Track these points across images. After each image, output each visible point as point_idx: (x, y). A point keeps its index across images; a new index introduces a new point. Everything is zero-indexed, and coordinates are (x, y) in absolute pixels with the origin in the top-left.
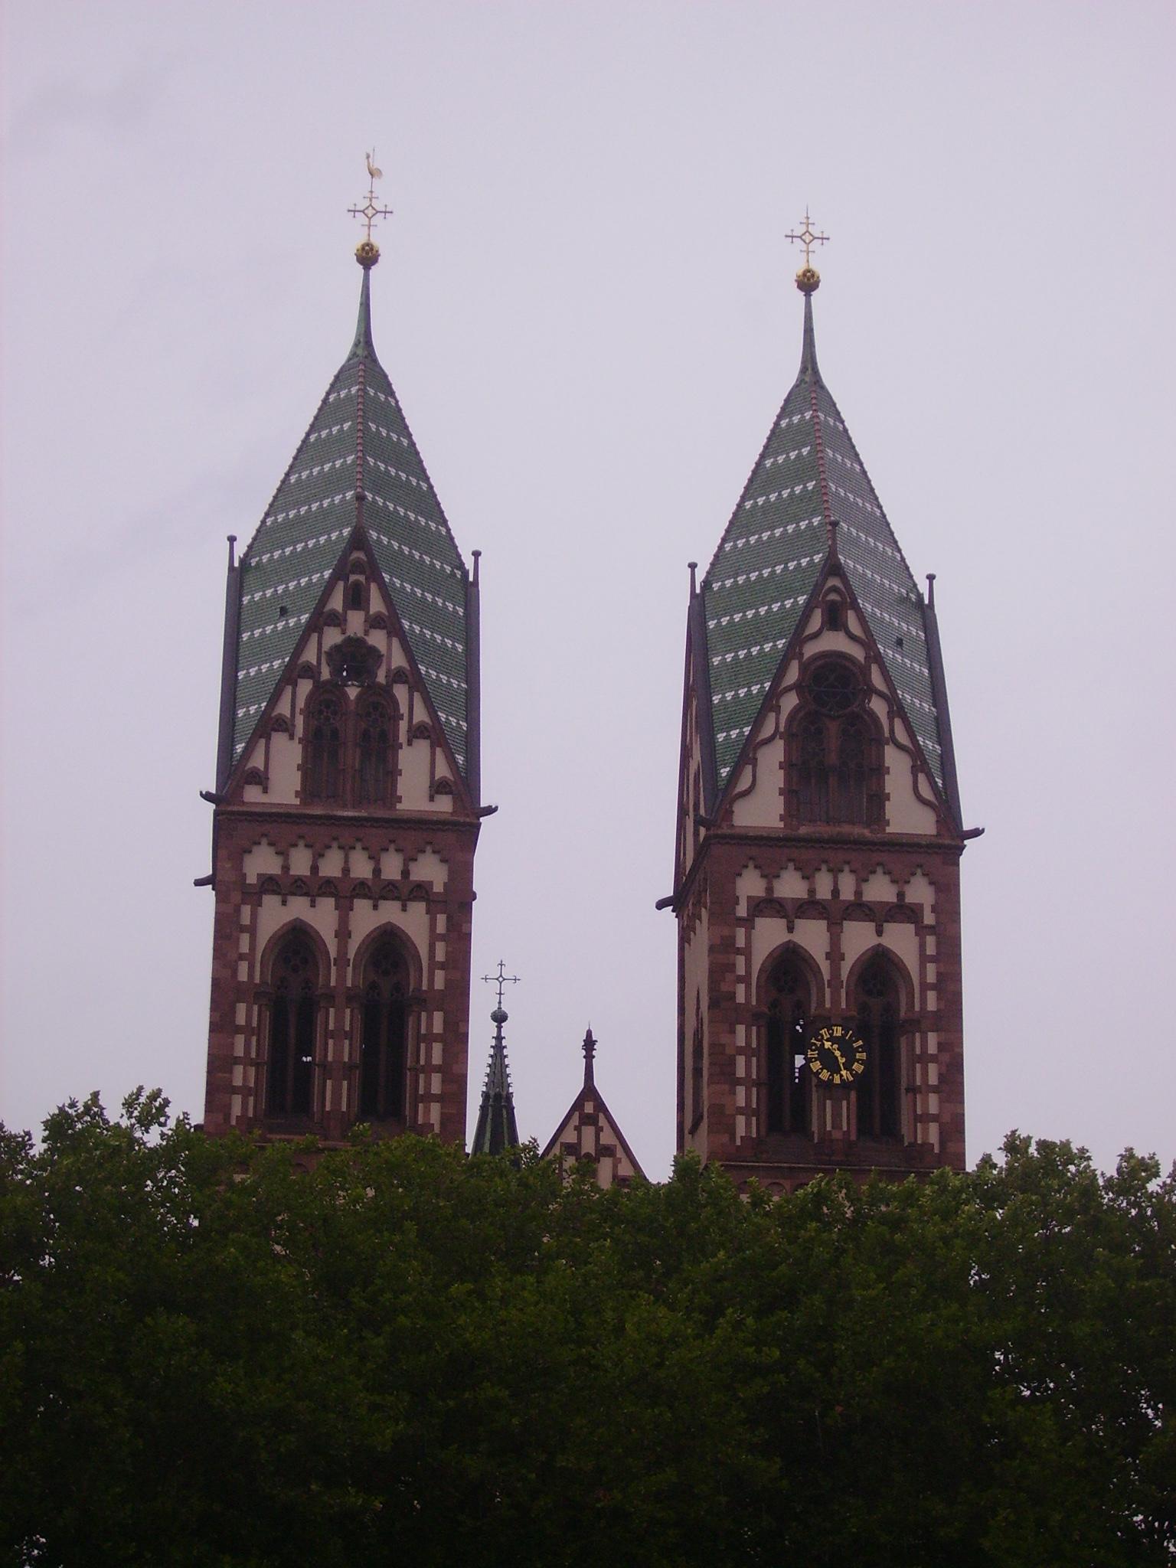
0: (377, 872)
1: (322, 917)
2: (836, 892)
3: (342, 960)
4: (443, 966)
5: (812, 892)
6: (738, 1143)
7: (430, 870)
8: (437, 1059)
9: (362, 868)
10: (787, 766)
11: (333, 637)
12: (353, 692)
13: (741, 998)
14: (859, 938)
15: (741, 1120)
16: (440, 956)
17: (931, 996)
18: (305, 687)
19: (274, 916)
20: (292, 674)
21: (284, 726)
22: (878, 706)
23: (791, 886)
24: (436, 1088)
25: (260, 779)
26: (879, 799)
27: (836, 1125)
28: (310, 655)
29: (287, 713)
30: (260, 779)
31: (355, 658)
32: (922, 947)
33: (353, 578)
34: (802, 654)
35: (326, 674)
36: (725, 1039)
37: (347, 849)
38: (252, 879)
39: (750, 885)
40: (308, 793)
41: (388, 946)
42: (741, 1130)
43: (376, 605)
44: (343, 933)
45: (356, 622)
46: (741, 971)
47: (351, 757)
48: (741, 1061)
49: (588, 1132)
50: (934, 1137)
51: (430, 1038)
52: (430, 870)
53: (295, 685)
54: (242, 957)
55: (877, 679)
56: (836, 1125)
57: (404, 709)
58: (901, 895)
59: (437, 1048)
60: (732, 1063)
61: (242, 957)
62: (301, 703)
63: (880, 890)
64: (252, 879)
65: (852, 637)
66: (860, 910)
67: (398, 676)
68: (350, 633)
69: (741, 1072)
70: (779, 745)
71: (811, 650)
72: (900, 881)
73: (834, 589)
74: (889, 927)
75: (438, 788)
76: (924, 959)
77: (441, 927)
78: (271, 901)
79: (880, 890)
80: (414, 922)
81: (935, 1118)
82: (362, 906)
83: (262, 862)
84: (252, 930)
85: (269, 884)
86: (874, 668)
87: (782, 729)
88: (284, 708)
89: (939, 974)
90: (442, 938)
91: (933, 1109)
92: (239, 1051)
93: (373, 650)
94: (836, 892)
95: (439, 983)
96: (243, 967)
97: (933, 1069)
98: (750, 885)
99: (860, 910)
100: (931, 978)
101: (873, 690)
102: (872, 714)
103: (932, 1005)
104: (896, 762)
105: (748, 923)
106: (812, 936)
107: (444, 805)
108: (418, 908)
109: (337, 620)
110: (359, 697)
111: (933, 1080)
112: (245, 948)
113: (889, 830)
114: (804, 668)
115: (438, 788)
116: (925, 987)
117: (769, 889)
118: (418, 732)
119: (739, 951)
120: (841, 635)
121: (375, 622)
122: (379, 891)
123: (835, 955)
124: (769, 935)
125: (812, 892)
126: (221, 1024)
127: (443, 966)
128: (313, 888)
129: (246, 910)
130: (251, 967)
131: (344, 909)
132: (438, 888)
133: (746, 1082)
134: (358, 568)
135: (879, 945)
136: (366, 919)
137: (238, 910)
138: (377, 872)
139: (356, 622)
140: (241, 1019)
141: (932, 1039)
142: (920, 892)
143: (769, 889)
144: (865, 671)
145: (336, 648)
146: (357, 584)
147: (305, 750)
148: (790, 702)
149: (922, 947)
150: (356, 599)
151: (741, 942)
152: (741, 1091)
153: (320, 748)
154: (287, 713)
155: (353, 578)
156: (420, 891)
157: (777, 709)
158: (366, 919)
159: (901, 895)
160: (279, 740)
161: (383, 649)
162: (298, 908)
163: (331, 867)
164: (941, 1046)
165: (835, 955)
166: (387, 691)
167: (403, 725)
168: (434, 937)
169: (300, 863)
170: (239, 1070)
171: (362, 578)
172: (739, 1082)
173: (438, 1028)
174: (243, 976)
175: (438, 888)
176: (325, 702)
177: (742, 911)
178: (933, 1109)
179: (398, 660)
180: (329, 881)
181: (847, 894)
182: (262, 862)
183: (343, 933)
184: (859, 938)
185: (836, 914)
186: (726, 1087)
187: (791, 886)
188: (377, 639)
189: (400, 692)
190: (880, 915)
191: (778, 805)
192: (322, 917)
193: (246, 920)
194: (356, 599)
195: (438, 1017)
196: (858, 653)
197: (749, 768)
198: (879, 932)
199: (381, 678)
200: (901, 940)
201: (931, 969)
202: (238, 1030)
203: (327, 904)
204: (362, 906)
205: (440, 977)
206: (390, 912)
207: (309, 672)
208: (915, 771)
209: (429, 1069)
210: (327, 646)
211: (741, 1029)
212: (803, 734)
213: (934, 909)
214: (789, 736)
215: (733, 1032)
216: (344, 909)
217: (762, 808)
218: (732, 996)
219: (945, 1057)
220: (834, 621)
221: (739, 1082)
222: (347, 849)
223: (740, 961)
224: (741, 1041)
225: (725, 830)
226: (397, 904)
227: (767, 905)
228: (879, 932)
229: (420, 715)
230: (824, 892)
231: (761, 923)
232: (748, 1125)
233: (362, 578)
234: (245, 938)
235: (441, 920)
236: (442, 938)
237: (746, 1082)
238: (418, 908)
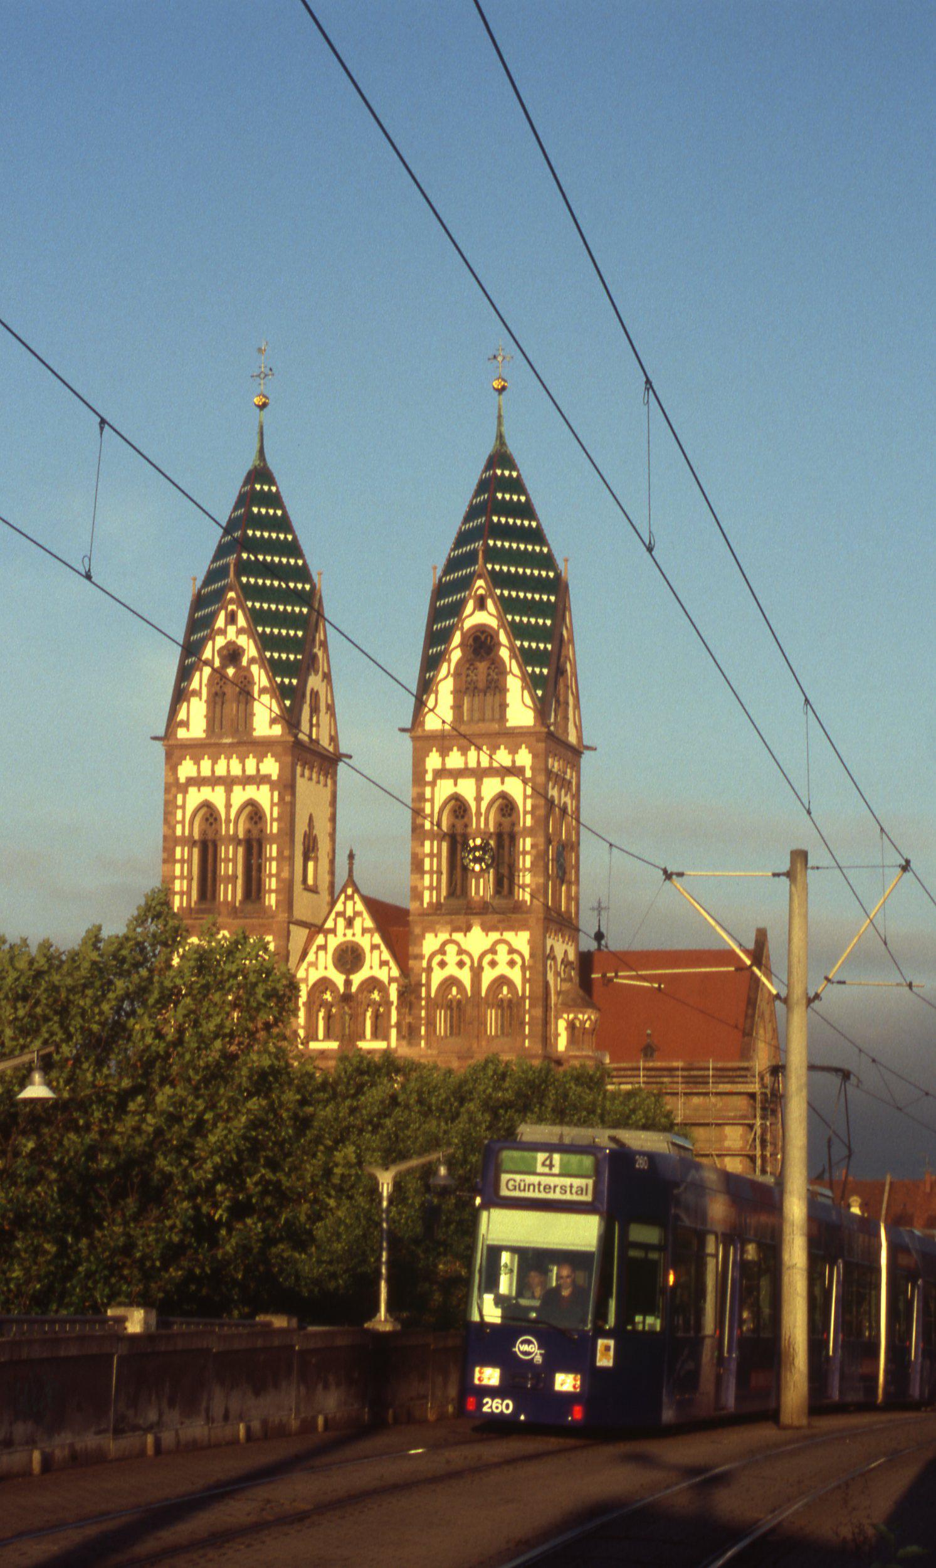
0: (244, 770)
1: (216, 796)
2: (479, 762)
3: (228, 821)
4: (276, 820)
5: (466, 763)
6: (425, 905)
7: (271, 767)
8: (274, 871)
9: (236, 769)
10: (458, 693)
11: (220, 641)
12: (231, 671)
13: (428, 825)
14: (492, 787)
15: (427, 894)
16: (275, 815)
17: (529, 817)
18: (207, 671)
19: (195, 797)
21: (196, 693)
22: (504, 653)
23: (455, 760)
24: (274, 886)
25: (185, 724)
26: (504, 706)
27: (477, 892)
28: (207, 654)
29: (198, 688)
30: (185, 724)
31: (232, 654)
32: (525, 790)
33: (230, 607)
34: (462, 627)
35: (217, 664)
36: (418, 850)
37: (228, 758)
38: (182, 780)
39: (433, 761)
41: (254, 811)
42: (426, 899)
43: (241, 621)
44: (228, 806)
45: (232, 630)
46: (428, 811)
47: (231, 708)
48: (427, 861)
49: (349, 904)
50: (528, 897)
51: (271, 859)
53: (201, 671)
54: (178, 822)
55: (503, 638)
56: (477, 892)
57: (256, 679)
58: (514, 761)
59: (274, 864)
60: (422, 862)
61: (178, 822)
62: (205, 681)
63: (503, 757)
64: (182, 780)
65: (491, 614)
66: (491, 772)
67: (252, 661)
68: (228, 639)
69: (427, 867)
70: (450, 680)
71: (468, 624)
72: (513, 751)
73: (480, 587)
74: (508, 779)
75: (273, 721)
76: (525, 797)
77: (276, 800)
78: (192, 790)
79: (503, 757)
80: (264, 796)
81: (528, 886)
82: (237, 789)
83: (187, 769)
84: (183, 807)
85: (191, 781)
86: (502, 632)
87: (452, 671)
88: (195, 685)
89: (533, 806)
90: (276, 804)
91: (528, 880)
92: (178, 873)
93: (241, 648)
94: (479, 762)
95: (275, 830)
96: (179, 828)
97: (528, 858)
99: (491, 772)
100: (529, 808)
101: (500, 644)
102: (502, 660)
103: (529, 823)
104: (514, 684)
105: (433, 784)
106: (466, 788)
107: (277, 730)
108: (265, 788)
109: (223, 632)
110: (235, 674)
111: (528, 865)
112: (179, 817)
113: (508, 725)
114: (463, 635)
115: (273, 721)
116: (525, 813)
117: (443, 763)
118: (263, 691)
119: (428, 800)
120: (484, 613)
121: (240, 631)
122: (246, 780)
123: (479, 799)
124: (445, 789)
125: (466, 763)
126: (169, 859)
127: (276, 820)
128: (213, 781)
129: (180, 797)
130: (184, 827)
131: (229, 792)
132: (275, 777)
133: (431, 872)
134: (231, 601)
135: (503, 791)
136: (240, 796)
137: (175, 798)
138: (244, 770)
139: (232, 630)
140: (178, 856)
141: (528, 841)
143: (443, 763)
144: (498, 633)
145: (222, 648)
146: (232, 611)
147: (208, 707)
148: (456, 655)
149: (525, 790)
150: (232, 619)
151: (428, 795)
152: (427, 877)
153: (216, 700)
154: (198, 688)
155: (230, 607)
157: (449, 661)
158: (240, 796)
159: (514, 761)
160: (194, 700)
161: (245, 647)
162: (206, 793)
163: (221, 769)
164: (533, 846)
165: (479, 799)
166: (247, 669)
167: (256, 689)
168: (273, 805)
169: (206, 771)
170: (177, 882)
171: (234, 607)
172: (427, 872)
173: (274, 854)
174: (179, 832)
175: (275, 777)
177: (429, 777)
178: (528, 880)
180: (220, 777)
181: (485, 763)
183: (228, 806)
184: (492, 787)
185: (479, 774)
186: (418, 876)
187: (455, 760)
188: (243, 641)
189: (255, 669)
190: (505, 772)
191: (449, 716)
192: (216, 796)
193: (180, 802)
194: (232, 619)
195: (274, 847)
196: (493, 623)
197: (433, 696)
198: (503, 782)
199: (244, 662)
200: (514, 788)
201: (529, 802)
202: (176, 861)
203: (220, 789)
204: (237, 789)
205: (275, 825)
206: (251, 792)
207: (207, 663)
208: (523, 689)
209: (271, 876)
210: (217, 647)
211: (427, 843)
213: (532, 768)
214: (457, 675)
215: (423, 845)
216: (229, 792)
218: (423, 825)
219: (534, 852)
220: (481, 605)
221: (427, 872)
222: (228, 758)
223: (428, 806)
224: (427, 850)
225: (419, 732)
226: (255, 787)
227: (442, 773)
228: (503, 782)
229: (265, 682)
230: (472, 764)
231: (438, 781)
232: (431, 896)
233: (234, 607)
234: (179, 813)
235: (276, 794)
236: (276, 804)
237: (431, 872)
238: (265, 788)
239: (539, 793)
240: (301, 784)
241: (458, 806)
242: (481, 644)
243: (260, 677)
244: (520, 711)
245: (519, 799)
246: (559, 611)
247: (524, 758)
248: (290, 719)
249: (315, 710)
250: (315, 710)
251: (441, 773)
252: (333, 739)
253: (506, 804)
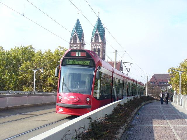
9: (76, 46)
20: (72, 37)
22: (99, 36)
23: (95, 45)
31: (75, 36)
40: (74, 42)
43: (76, 33)
52: (79, 45)
79: (99, 45)
83: (71, 46)
98: (93, 45)
104: (100, 38)
106: (96, 47)
142: (101, 45)
156: (78, 46)
176: (74, 38)
179: (77, 35)
182: (71, 46)
184: (98, 47)
194: (75, 33)
200: (100, 47)
212: (95, 37)
217: (93, 41)
220: (97, 31)
227: (93, 46)
239: (102, 48)
240: (81, 47)
241: (95, 49)
242: (97, 35)
243: (78, 38)
244: (100, 41)
245: (100, 48)
246: (104, 32)
247: (101, 45)
248: (80, 41)
249: (82, 40)
250: (82, 40)
251: (93, 46)
252: (84, 43)
253: (99, 49)
